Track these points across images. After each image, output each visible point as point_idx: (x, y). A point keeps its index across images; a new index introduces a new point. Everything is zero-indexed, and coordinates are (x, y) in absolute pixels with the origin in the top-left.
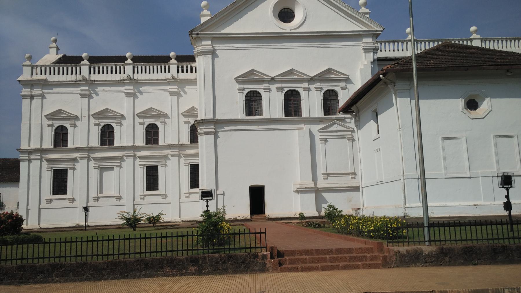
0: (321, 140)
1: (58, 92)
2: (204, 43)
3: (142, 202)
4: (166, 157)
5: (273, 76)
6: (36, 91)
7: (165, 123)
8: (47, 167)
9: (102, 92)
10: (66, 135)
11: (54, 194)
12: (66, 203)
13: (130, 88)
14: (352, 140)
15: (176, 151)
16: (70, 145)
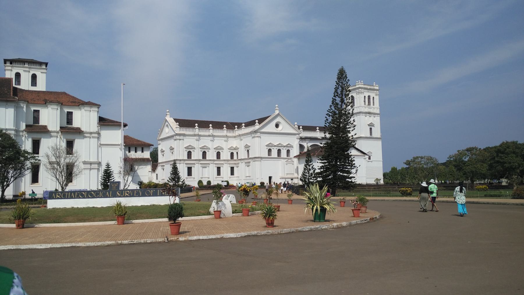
0: (286, 164)
1: (189, 138)
2: (258, 134)
3: (230, 179)
4: (223, 164)
5: (275, 145)
6: (181, 137)
7: (222, 151)
8: (185, 166)
9: (202, 139)
10: (191, 154)
11: (188, 176)
12: (192, 179)
13: (211, 138)
14: (293, 164)
15: (226, 162)
16: (193, 158)
